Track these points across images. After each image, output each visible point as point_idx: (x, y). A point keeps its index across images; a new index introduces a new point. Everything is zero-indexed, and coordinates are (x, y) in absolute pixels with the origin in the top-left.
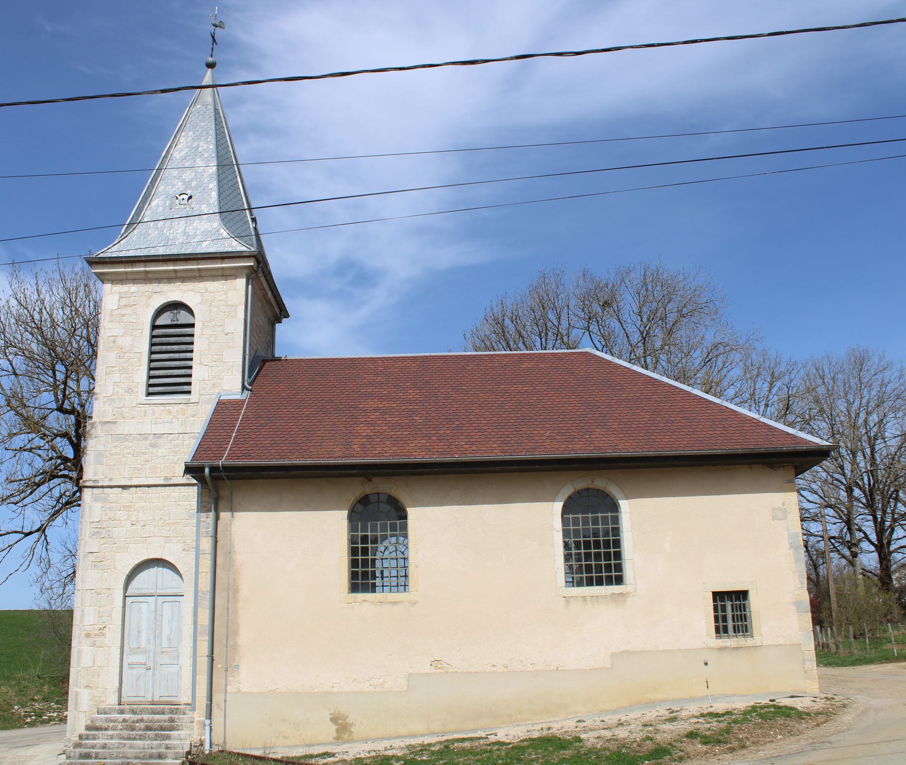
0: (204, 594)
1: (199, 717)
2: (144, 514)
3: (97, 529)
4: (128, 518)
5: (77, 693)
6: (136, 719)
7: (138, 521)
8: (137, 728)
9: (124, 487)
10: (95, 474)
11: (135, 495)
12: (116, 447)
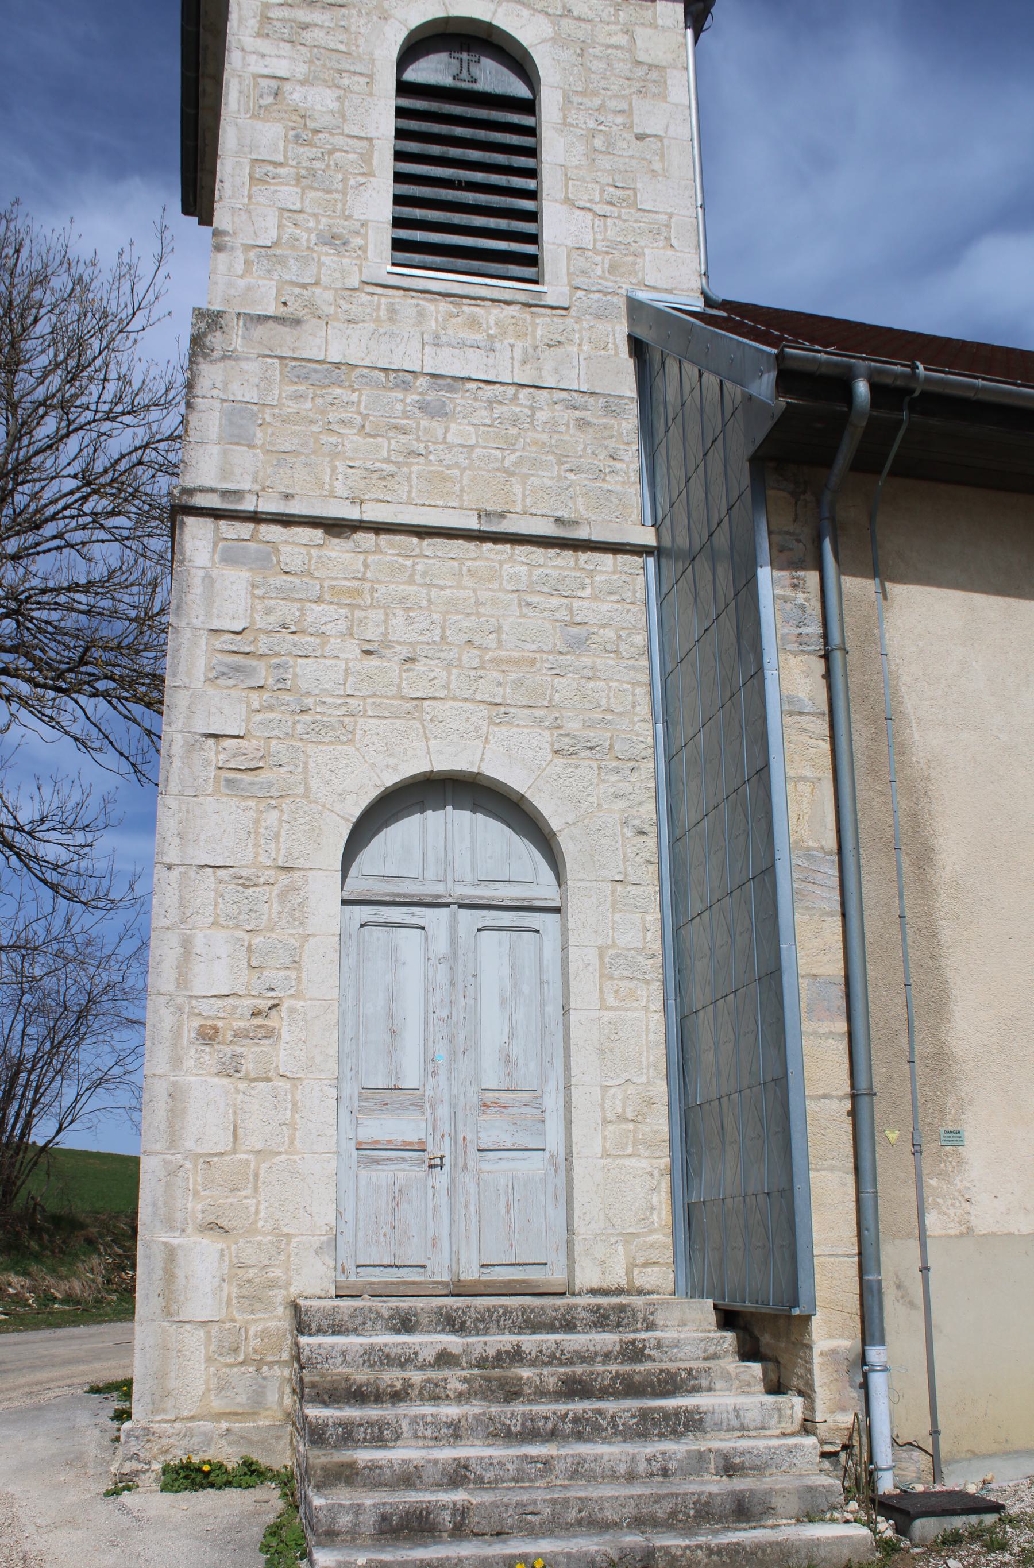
0: (809, 857)
1: (831, 1336)
2: (409, 621)
3: (236, 658)
4: (350, 629)
5: (171, 1254)
6: (492, 1352)
7: (386, 644)
8: (527, 1390)
9: (335, 527)
10: (225, 473)
11: (371, 559)
12: (298, 397)
